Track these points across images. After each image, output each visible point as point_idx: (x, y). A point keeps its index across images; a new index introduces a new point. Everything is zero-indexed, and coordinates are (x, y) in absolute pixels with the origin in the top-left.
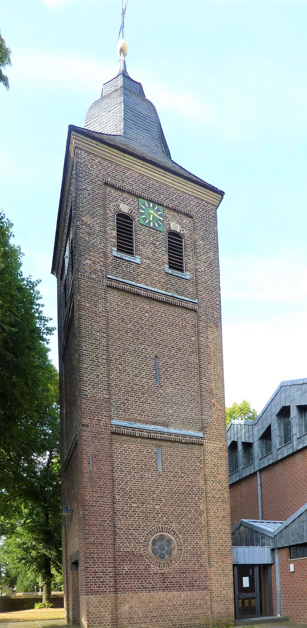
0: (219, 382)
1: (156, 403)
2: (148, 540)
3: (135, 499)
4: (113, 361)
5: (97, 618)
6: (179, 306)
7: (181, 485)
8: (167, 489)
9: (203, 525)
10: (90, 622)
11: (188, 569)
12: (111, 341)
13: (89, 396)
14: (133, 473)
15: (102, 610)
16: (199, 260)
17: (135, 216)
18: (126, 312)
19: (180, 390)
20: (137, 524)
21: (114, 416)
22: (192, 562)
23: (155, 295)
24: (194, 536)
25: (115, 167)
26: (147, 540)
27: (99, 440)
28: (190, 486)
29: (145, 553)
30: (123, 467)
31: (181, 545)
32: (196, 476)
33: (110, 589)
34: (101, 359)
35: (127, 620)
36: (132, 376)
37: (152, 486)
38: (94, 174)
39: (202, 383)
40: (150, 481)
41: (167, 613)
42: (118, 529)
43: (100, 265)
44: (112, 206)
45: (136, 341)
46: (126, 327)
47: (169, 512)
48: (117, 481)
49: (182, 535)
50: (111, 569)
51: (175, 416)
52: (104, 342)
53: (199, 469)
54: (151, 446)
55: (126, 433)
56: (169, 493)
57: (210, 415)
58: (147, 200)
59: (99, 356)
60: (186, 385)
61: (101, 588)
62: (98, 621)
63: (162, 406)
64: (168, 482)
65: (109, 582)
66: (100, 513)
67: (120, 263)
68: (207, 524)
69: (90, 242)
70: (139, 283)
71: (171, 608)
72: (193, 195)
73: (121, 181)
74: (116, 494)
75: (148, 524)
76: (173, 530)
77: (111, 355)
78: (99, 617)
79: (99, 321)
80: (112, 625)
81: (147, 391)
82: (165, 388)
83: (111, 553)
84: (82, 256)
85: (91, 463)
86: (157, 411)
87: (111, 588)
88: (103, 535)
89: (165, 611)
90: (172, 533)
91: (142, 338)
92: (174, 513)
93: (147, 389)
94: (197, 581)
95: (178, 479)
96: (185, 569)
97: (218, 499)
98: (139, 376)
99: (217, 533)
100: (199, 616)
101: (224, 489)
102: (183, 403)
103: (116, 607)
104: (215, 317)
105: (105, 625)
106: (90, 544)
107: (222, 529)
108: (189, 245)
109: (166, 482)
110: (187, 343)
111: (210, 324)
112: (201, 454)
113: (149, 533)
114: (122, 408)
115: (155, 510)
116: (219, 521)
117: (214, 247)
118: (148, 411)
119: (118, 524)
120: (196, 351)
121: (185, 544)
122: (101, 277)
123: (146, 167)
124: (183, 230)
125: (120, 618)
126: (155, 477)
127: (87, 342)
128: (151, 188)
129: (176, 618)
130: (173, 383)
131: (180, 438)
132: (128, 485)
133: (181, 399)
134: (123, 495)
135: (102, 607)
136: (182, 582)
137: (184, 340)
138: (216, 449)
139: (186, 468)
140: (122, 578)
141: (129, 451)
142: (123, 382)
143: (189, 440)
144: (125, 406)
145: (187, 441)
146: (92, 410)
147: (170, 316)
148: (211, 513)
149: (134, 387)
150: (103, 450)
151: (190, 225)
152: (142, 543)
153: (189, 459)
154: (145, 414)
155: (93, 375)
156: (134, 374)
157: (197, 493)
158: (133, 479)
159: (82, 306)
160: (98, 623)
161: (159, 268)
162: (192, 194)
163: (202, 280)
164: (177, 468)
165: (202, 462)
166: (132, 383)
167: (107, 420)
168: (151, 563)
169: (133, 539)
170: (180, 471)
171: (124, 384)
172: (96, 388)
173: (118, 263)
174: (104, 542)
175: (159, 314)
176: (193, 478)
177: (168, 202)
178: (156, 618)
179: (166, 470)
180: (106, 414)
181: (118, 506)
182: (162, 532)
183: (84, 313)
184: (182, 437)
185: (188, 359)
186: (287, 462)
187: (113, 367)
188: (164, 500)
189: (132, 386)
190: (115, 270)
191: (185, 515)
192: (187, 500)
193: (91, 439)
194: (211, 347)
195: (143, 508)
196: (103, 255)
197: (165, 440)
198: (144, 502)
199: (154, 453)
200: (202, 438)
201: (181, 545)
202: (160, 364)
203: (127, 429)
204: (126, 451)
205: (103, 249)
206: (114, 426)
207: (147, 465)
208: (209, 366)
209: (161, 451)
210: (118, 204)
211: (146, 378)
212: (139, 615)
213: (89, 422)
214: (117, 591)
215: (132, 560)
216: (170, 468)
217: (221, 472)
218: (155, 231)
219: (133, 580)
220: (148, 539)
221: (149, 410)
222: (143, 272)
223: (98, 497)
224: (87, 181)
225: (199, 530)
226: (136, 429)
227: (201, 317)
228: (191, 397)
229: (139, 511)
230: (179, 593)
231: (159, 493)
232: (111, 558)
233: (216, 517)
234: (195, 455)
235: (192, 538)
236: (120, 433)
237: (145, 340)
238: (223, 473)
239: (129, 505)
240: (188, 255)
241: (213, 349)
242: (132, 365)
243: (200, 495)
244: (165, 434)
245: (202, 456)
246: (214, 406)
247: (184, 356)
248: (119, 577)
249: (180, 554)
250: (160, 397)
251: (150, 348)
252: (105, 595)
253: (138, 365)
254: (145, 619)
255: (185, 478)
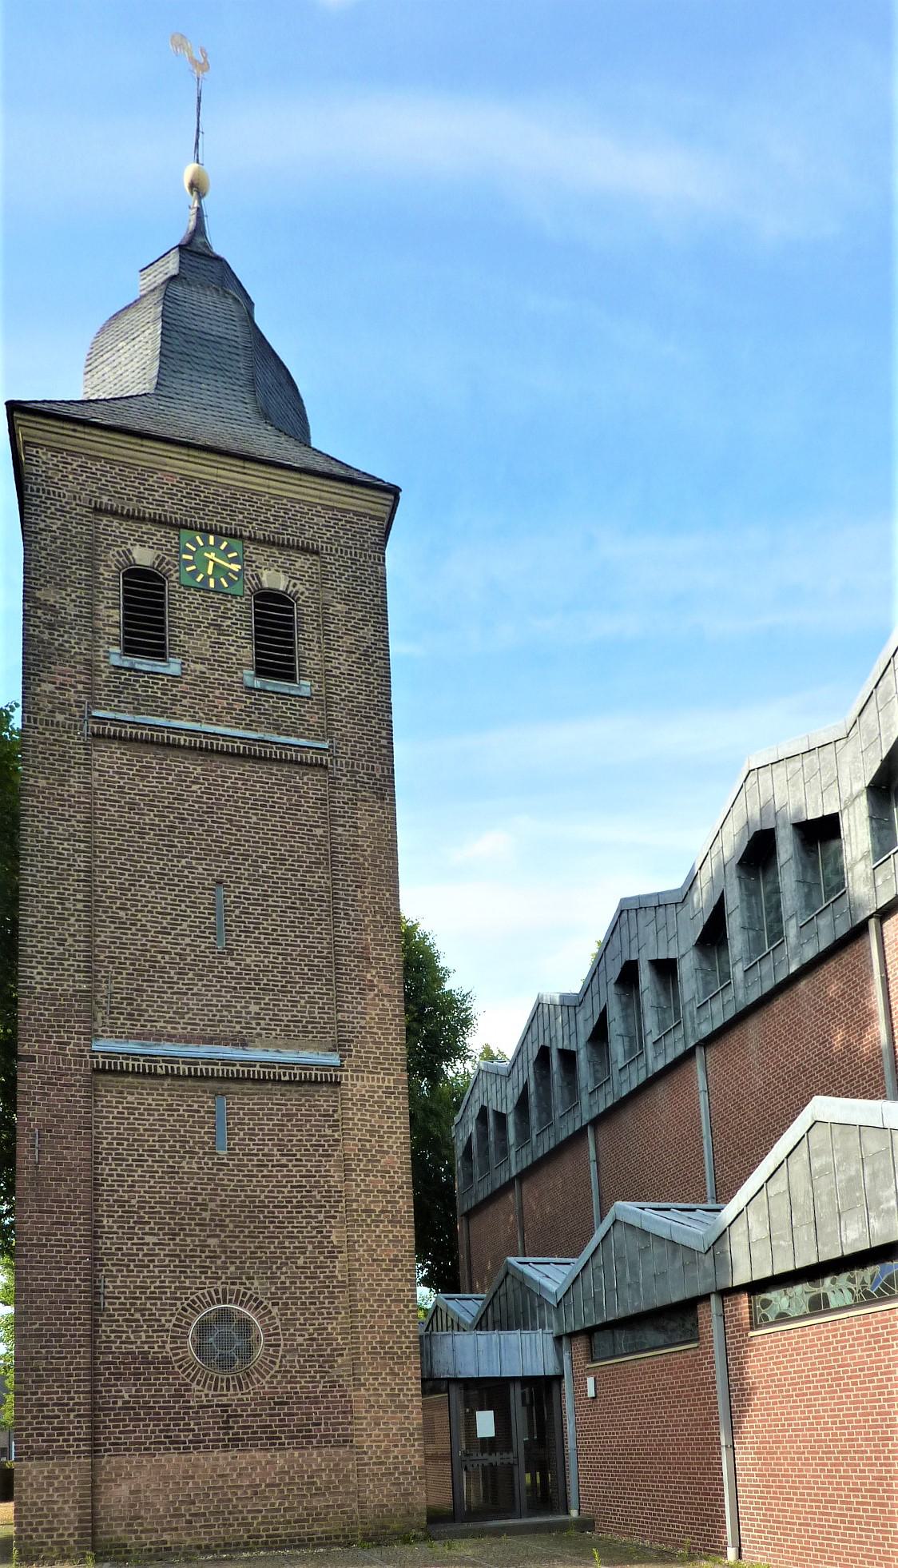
0: (385, 929)
1: (216, 991)
2: (187, 1323)
3: (152, 1225)
4: (105, 902)
5: (40, 1516)
6: (280, 761)
7: (279, 1187)
8: (239, 1196)
9: (338, 1282)
10: (24, 1527)
11: (296, 1393)
12: (100, 857)
13: (38, 990)
14: (150, 1163)
15: (55, 1498)
16: (335, 650)
17: (170, 570)
18: (141, 787)
19: (280, 957)
20: (158, 1284)
21: (103, 1031)
22: (307, 1375)
23: (215, 742)
24: (313, 1310)
25: (120, 470)
26: (183, 1324)
27: (61, 1090)
28: (305, 1186)
29: (178, 1354)
30: (123, 1149)
31: (278, 1334)
32: (321, 1161)
33: (78, 1446)
34: (71, 901)
35: (124, 1523)
36: (152, 933)
37: (199, 1191)
38: (67, 494)
39: (338, 936)
40: (195, 1181)
41: (235, 1507)
42: (105, 1298)
43: (76, 692)
44: (113, 555)
45: (165, 852)
46: (141, 821)
47: (245, 1253)
48: (105, 1183)
49: (279, 1310)
50: (82, 1396)
51: (264, 1019)
52: (81, 861)
53: (331, 1143)
54: (200, 1094)
55: (130, 1069)
56: (246, 1206)
57: (359, 1009)
58: (201, 530)
59: (66, 896)
60: (299, 943)
61: (55, 1444)
62: (45, 1526)
63: (232, 997)
64: (243, 1181)
65: (76, 1428)
66: (57, 1262)
67: (130, 680)
68: (349, 1280)
69: (53, 644)
70: (177, 719)
71: (246, 1493)
72: (321, 502)
73: (135, 499)
74: (103, 1216)
75: (187, 1284)
76: (255, 1296)
77: (100, 889)
78: (46, 1516)
79: (70, 816)
80: (81, 1535)
81: (192, 965)
82: (241, 955)
83: (84, 1358)
84: (32, 677)
85: (37, 1145)
86: (218, 1011)
87: (81, 1443)
88: (65, 1313)
89: (230, 1500)
90: (252, 1305)
91: (181, 842)
92: (259, 1255)
93: (192, 960)
94: (320, 1424)
95: (272, 1171)
96: (287, 1393)
97: (379, 1216)
98: (173, 932)
99: (375, 1301)
100: (327, 1514)
101: (396, 1188)
102: (289, 985)
103: (94, 1489)
104: (378, 777)
105: (62, 1535)
106: (30, 1336)
107: (390, 1290)
108: (309, 615)
109: (239, 1181)
110: (302, 843)
111: (364, 793)
112: (336, 1106)
113: (188, 1305)
114: (126, 1009)
115: (207, 1249)
116: (383, 1270)
117: (375, 613)
118: (195, 1011)
119: (105, 1287)
120: (327, 860)
121: (288, 1330)
122: (77, 718)
123: (197, 461)
124: (295, 585)
125: (104, 1519)
126: (208, 1169)
127: (37, 866)
128: (211, 502)
129: (260, 1519)
130: (262, 940)
131: (277, 1070)
132: (134, 1192)
133: (282, 977)
134: (123, 1217)
135: (57, 1490)
136: (276, 1426)
137: (294, 837)
138: (375, 1092)
139: (294, 1142)
140: (112, 1417)
141: (141, 1111)
142: (129, 949)
143: (301, 1074)
144: (132, 1004)
145: (295, 1077)
146: (45, 1020)
147: (258, 785)
148: (358, 1251)
149: (159, 959)
150: (70, 1112)
151: (314, 571)
152: (168, 1331)
153: (301, 1120)
154: (185, 1021)
155: (51, 941)
156: (159, 929)
157: (323, 1203)
158: (150, 1177)
159: (28, 788)
160: (44, 1530)
161: (229, 679)
162: (317, 501)
163: (343, 694)
164: (268, 1145)
165: (337, 1126)
166: (153, 950)
167: (82, 1042)
168: (192, 1380)
169: (144, 1321)
170: (278, 1150)
171: (131, 954)
172: (57, 969)
173: (125, 679)
174: (66, 1330)
175: (227, 782)
176: (312, 1166)
177: (253, 528)
178: (202, 1519)
179: (237, 1151)
180: (80, 1027)
181: (105, 1244)
182: (225, 1303)
183: (32, 801)
184: (280, 1068)
185: (302, 880)
186: (643, 1103)
187: (104, 918)
188: (231, 1225)
189: (151, 956)
190: (115, 696)
191: (287, 1258)
192: (295, 1221)
193: (39, 1088)
194: (365, 848)
195: (175, 1245)
196: (85, 669)
197: (237, 1079)
198: (177, 1231)
199: (207, 1112)
200: (336, 1068)
201: (278, 1334)
202: (228, 900)
203: (134, 1060)
204: (131, 1110)
205: (85, 655)
206: (100, 1055)
207: (188, 1142)
208: (359, 894)
209: (228, 1104)
210: (129, 550)
211: (190, 936)
212: (158, 1510)
213: (36, 1048)
214: (100, 1451)
215: (141, 1374)
216: (249, 1145)
217: (390, 1147)
218: (220, 597)
219: (141, 1423)
220: (184, 1320)
221: (197, 1009)
222: (187, 693)
223: (53, 1224)
224: (49, 511)
225: (326, 1294)
226: (158, 1058)
227: (339, 779)
228: (309, 970)
229: (162, 1253)
230: (269, 1454)
231: (219, 1209)
232: (82, 1369)
233: (374, 1260)
234: (319, 1111)
235: (307, 1316)
236: (115, 1071)
237: (190, 848)
238: (395, 1149)
239: (135, 1241)
240: (305, 639)
241: (371, 851)
242: (153, 907)
243: (331, 1207)
244: (234, 1065)
245: (340, 1112)
246: (372, 987)
247: (292, 875)
248: (105, 1415)
249: (272, 1356)
250: (226, 978)
251: (201, 864)
252: (66, 1461)
253: (170, 907)
254: (174, 1520)
255: (290, 1168)
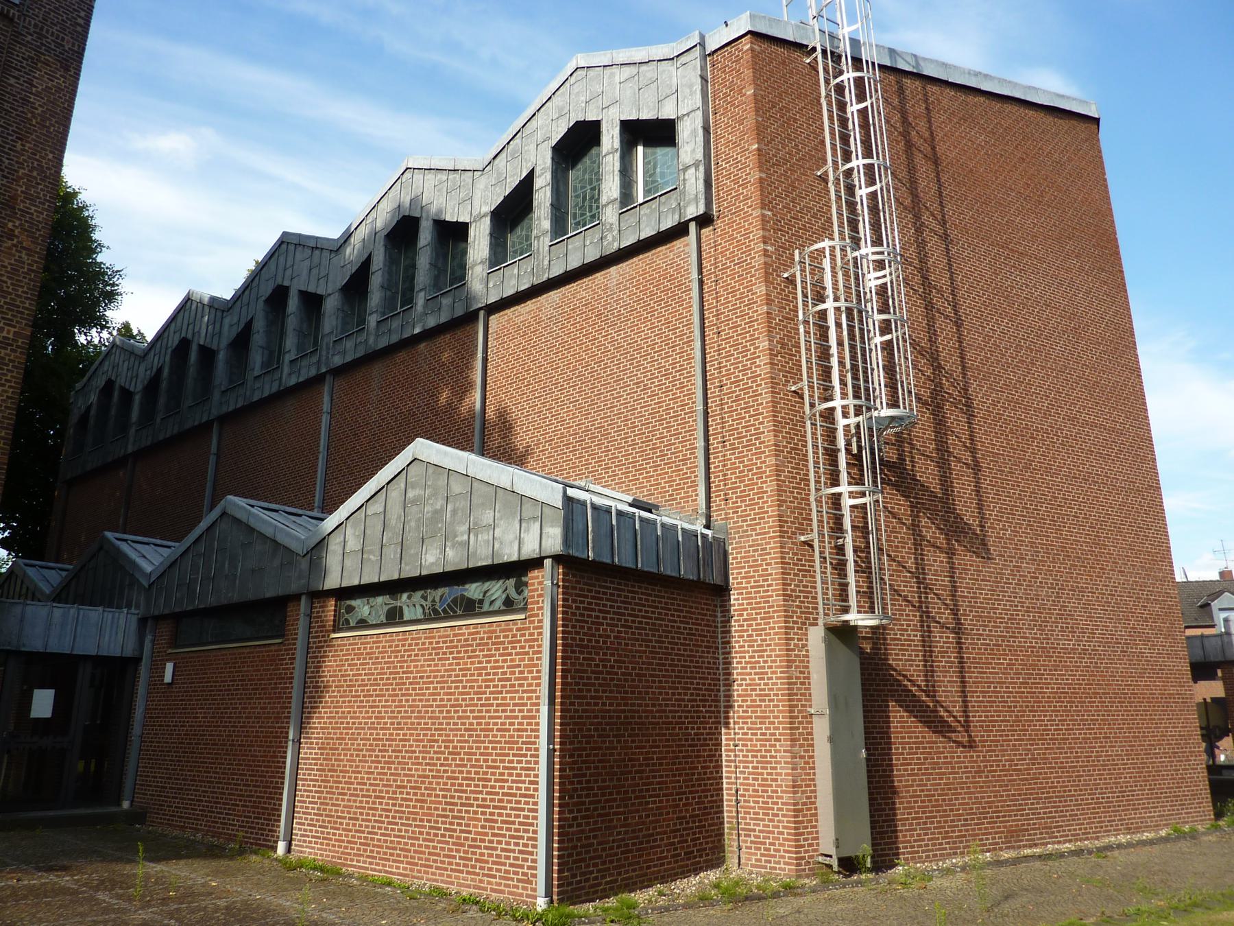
246: (11, 236)
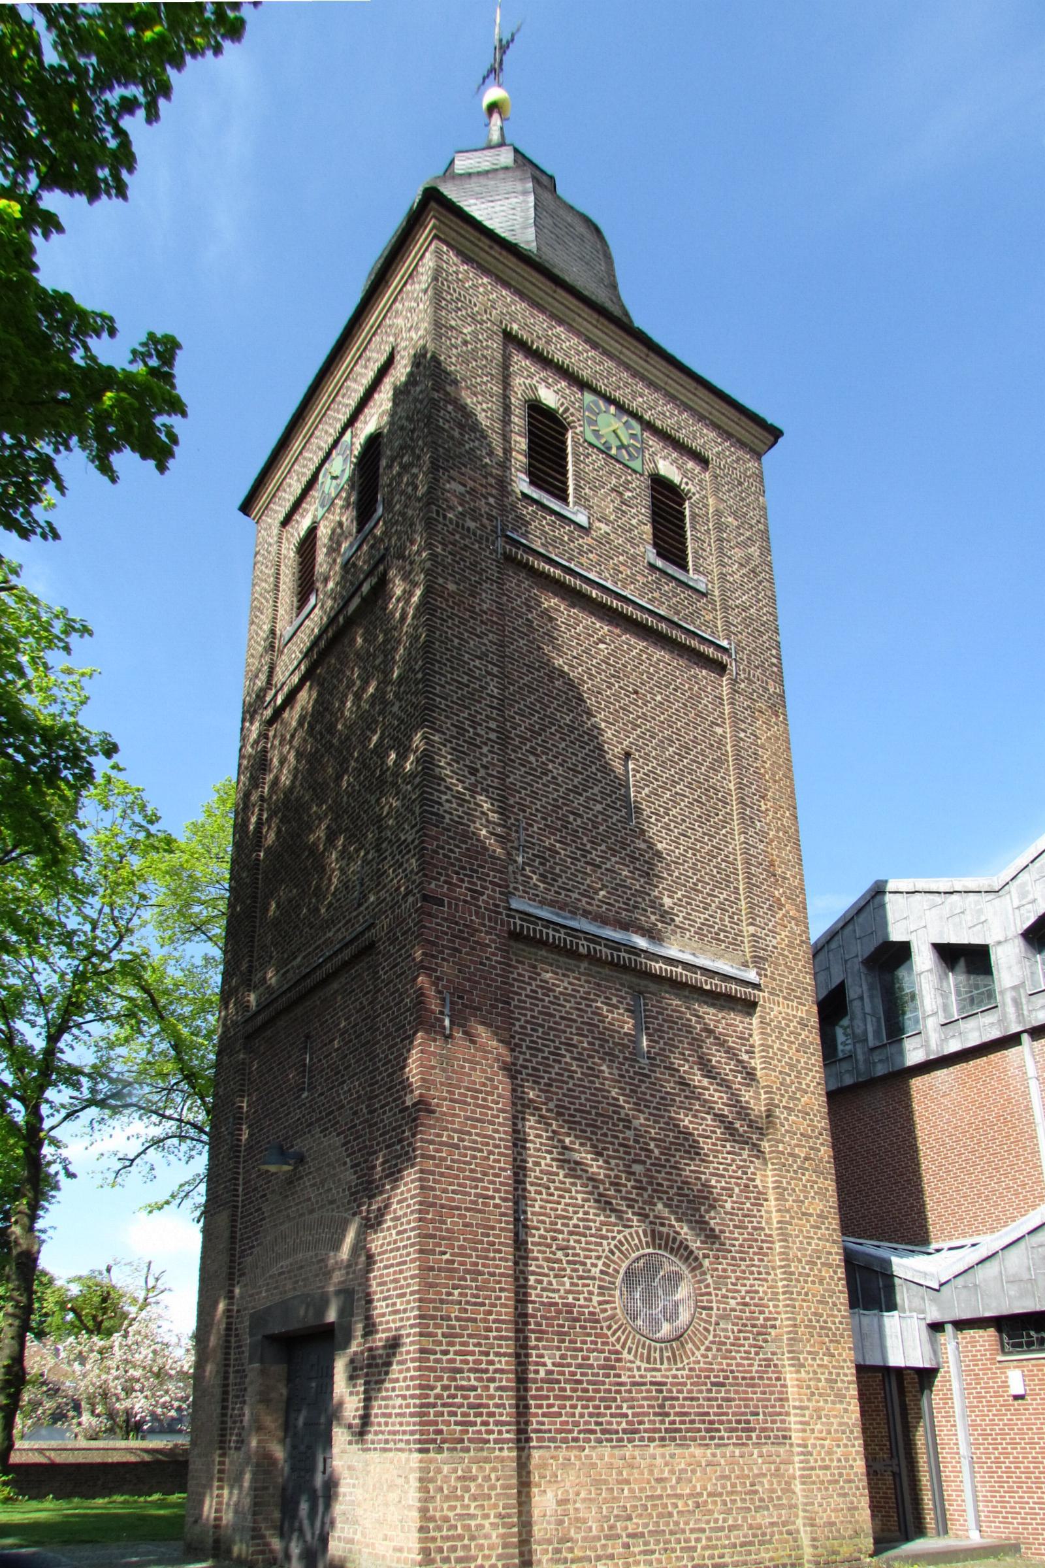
9: (766, 1235)
11: (732, 1372)
13: (447, 821)
15: (472, 1511)
20: (581, 1215)
26: (611, 1271)
27: (474, 949)
29: (605, 1310)
31: (709, 1294)
33: (500, 1432)
35: (550, 1548)
41: (677, 1523)
49: (711, 1263)
50: (503, 1359)
61: (471, 1429)
62: (461, 1553)
65: (497, 1406)
66: (472, 1171)
83: (505, 1306)
87: (504, 1429)
88: (482, 1242)
92: (686, 1192)
94: (758, 1414)
100: (772, 1534)
106: (440, 1269)
116: (812, 1226)
121: (720, 1289)
126: (630, 1078)
129: (704, 1542)
152: (594, 1278)
168: (623, 1347)
169: (569, 1262)
174: (484, 1265)
178: (641, 1541)
180: (495, 877)
201: (709, 1294)
203: (554, 930)
212: (590, 1528)
215: (566, 1334)
219: (568, 1403)
220: (613, 1266)
230: (709, 1451)
235: (738, 1274)
252: (485, 1454)
254: (610, 1543)
